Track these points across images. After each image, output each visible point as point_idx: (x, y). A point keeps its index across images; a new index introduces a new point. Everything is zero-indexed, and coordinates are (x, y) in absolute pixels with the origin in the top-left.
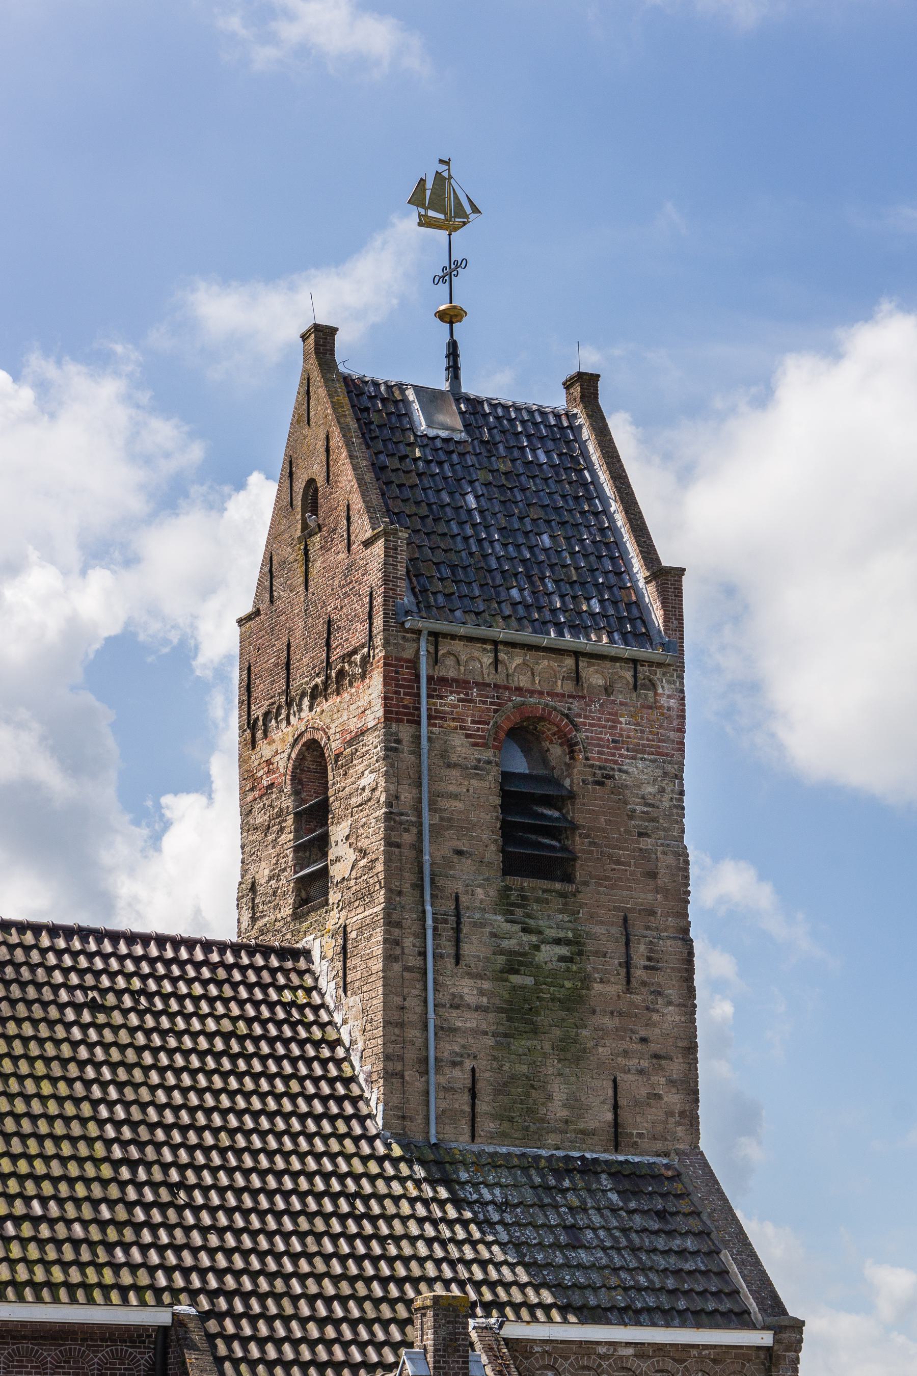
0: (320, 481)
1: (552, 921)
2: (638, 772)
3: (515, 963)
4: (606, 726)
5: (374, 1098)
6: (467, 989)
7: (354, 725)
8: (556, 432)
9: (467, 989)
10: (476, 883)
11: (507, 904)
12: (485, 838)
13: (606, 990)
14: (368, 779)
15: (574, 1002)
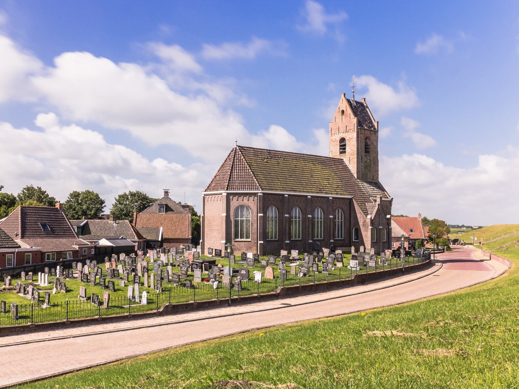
0: (345, 110)
1: (368, 158)
2: (375, 143)
3: (366, 162)
4: (373, 138)
5: (355, 175)
6: (362, 164)
7: (351, 137)
8: (362, 104)
9: (362, 164)
10: (363, 154)
11: (365, 156)
12: (364, 149)
13: (372, 165)
14: (353, 143)
15: (370, 166)
